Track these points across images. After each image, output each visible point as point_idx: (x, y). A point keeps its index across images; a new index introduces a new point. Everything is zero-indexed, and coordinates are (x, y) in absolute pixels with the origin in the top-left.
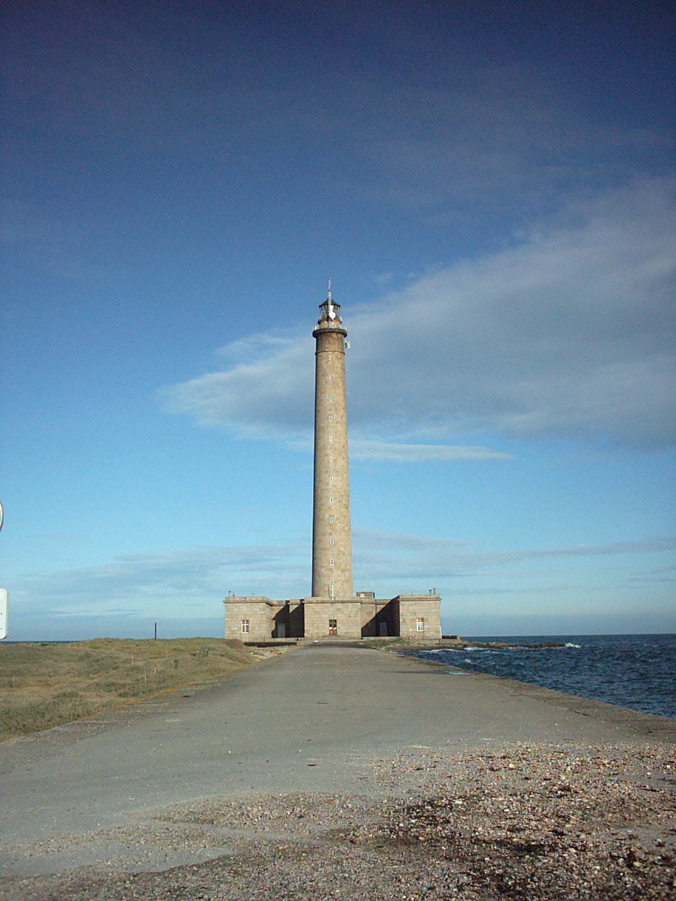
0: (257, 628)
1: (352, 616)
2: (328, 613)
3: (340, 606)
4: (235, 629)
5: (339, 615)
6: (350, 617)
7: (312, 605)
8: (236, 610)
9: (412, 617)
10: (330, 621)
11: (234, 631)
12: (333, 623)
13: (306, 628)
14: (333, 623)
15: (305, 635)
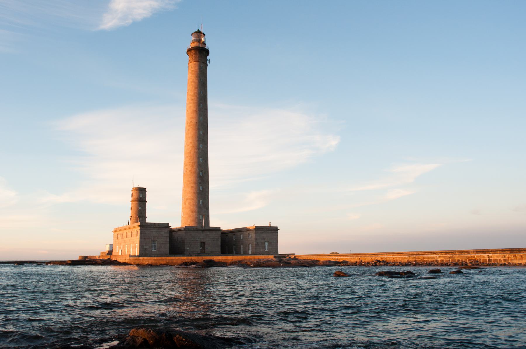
0: (163, 247)
1: (215, 240)
2: (200, 237)
3: (208, 233)
4: (147, 247)
5: (207, 239)
6: (214, 240)
7: (190, 231)
8: (147, 232)
9: (262, 241)
10: (201, 243)
11: (146, 249)
12: (203, 244)
13: (185, 248)
14: (203, 244)
15: (185, 253)
